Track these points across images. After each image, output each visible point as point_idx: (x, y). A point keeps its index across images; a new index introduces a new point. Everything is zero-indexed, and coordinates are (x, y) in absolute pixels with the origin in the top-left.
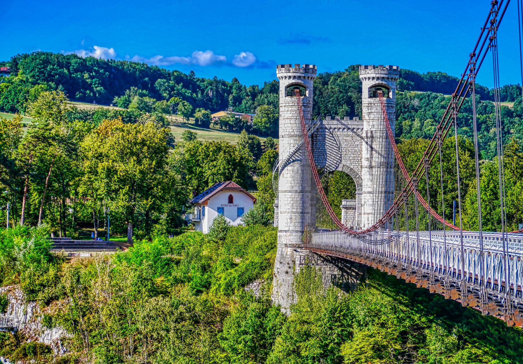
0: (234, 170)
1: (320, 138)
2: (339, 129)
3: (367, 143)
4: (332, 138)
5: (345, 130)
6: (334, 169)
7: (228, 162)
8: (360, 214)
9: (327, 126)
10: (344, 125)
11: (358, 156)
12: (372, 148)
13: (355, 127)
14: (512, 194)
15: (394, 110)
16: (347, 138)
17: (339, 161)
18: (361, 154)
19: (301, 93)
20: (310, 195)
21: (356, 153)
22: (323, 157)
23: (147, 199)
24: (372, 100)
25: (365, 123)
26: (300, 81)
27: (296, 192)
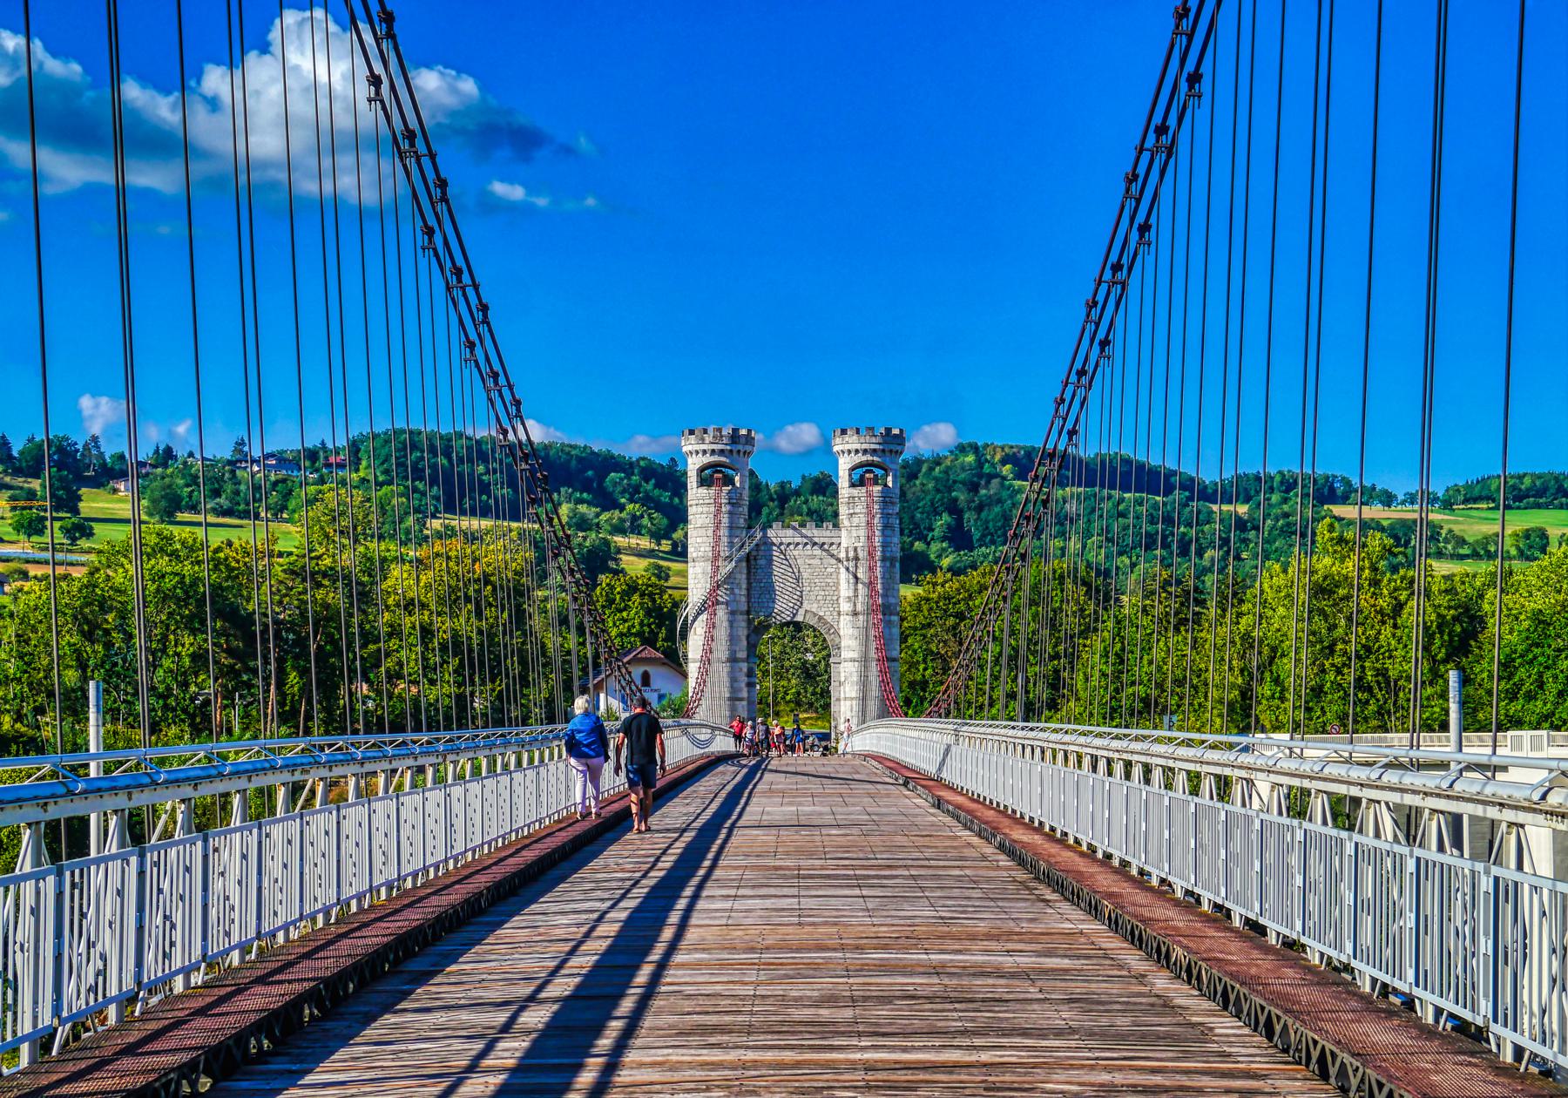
0: (659, 626)
7: (648, 613)
8: (838, 700)
12: (856, 577)
14: (1150, 663)
15: (897, 509)
18: (837, 589)
19: (728, 481)
20: (744, 666)
24: (855, 492)
25: (844, 533)
26: (723, 459)
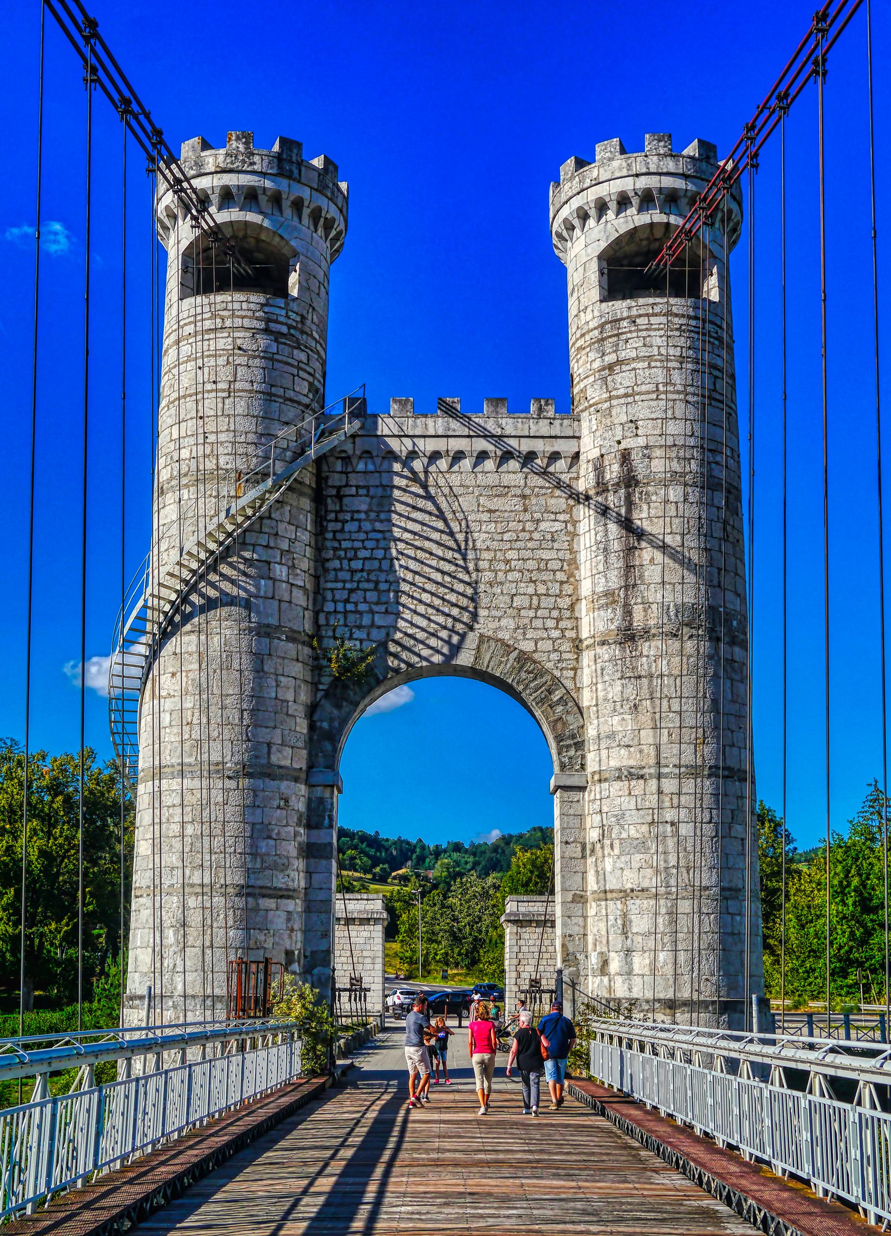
1: (362, 504)
2: (459, 456)
3: (604, 511)
4: (421, 503)
6: (437, 659)
8: (580, 899)
9: (394, 444)
10: (487, 436)
11: (555, 589)
13: (539, 446)
16: (497, 503)
17: (466, 617)
18: (571, 578)
20: (299, 796)
21: (545, 576)
22: (372, 596)
23: (59, 920)
24: (620, 307)
25: (588, 425)
26: (253, 217)
27: (217, 770)
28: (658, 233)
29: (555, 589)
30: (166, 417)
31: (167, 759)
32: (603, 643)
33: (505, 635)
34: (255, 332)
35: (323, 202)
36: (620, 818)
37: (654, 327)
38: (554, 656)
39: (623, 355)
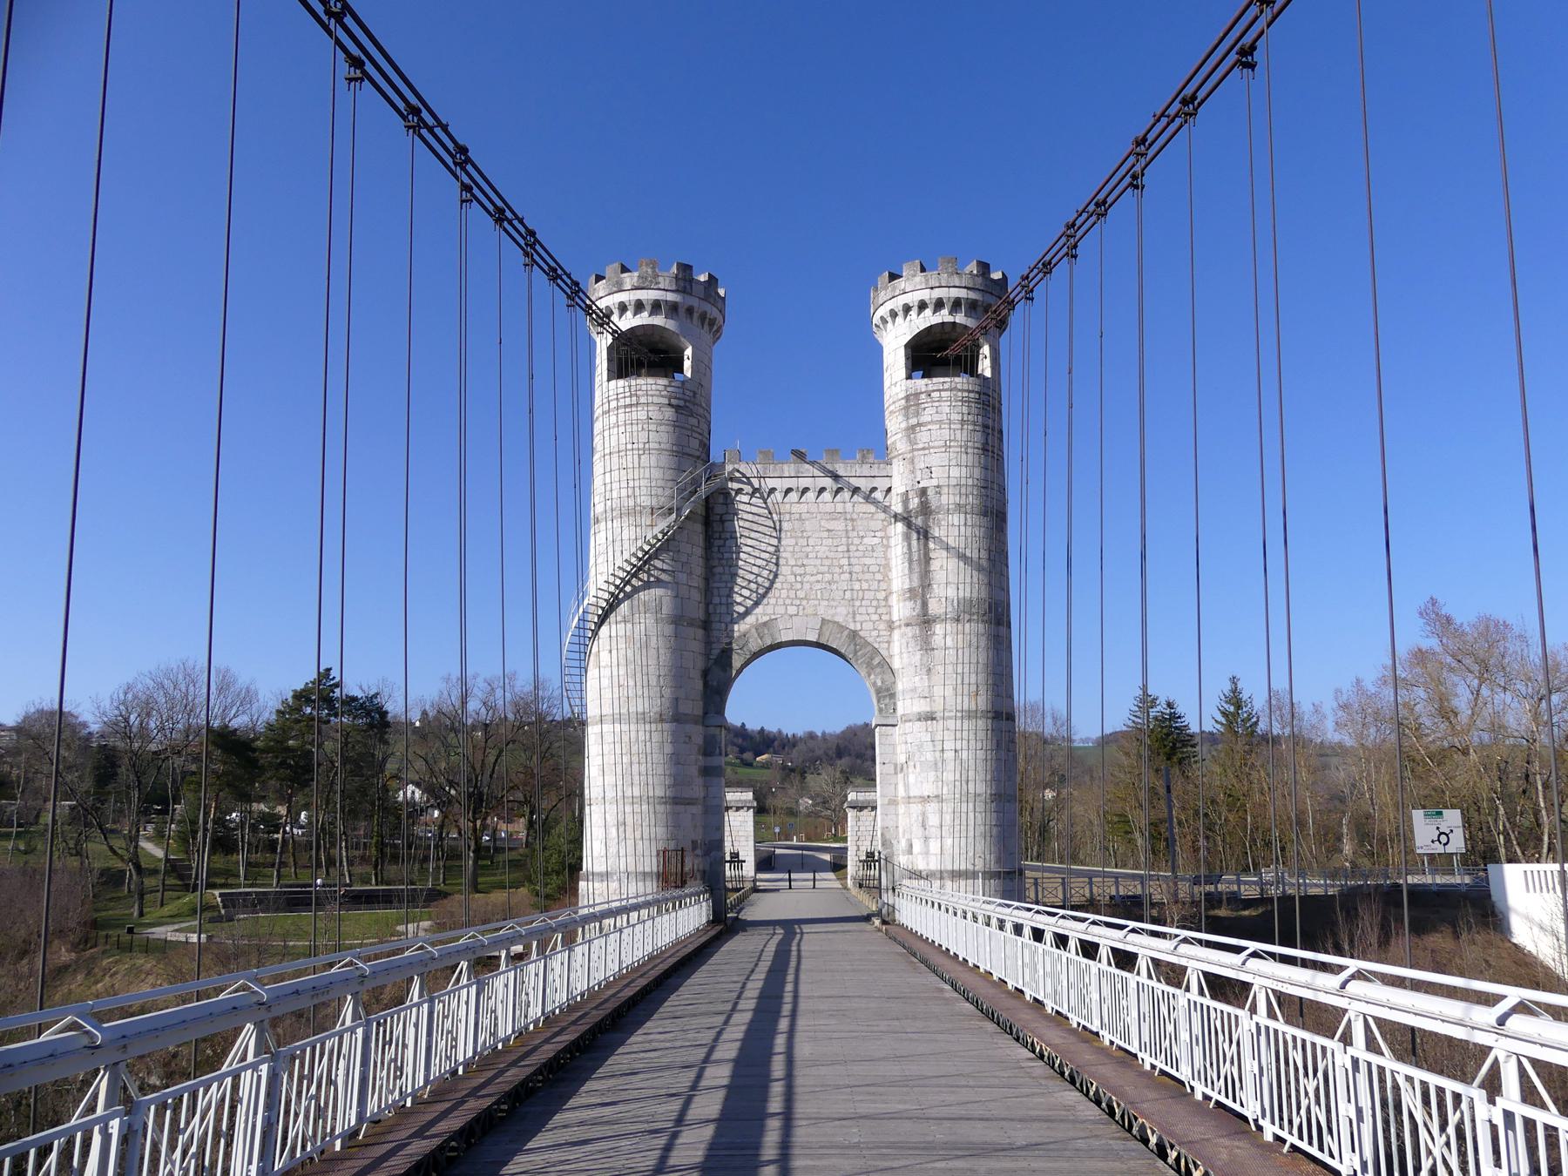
5: (827, 496)
11: (875, 585)
18: (886, 578)
21: (867, 576)
24: (921, 383)
28: (948, 329)
29: (875, 585)
30: (598, 468)
31: (607, 710)
32: (907, 625)
33: (839, 619)
34: (660, 405)
35: (707, 307)
36: (920, 746)
37: (945, 398)
38: (875, 633)
39: (923, 419)
